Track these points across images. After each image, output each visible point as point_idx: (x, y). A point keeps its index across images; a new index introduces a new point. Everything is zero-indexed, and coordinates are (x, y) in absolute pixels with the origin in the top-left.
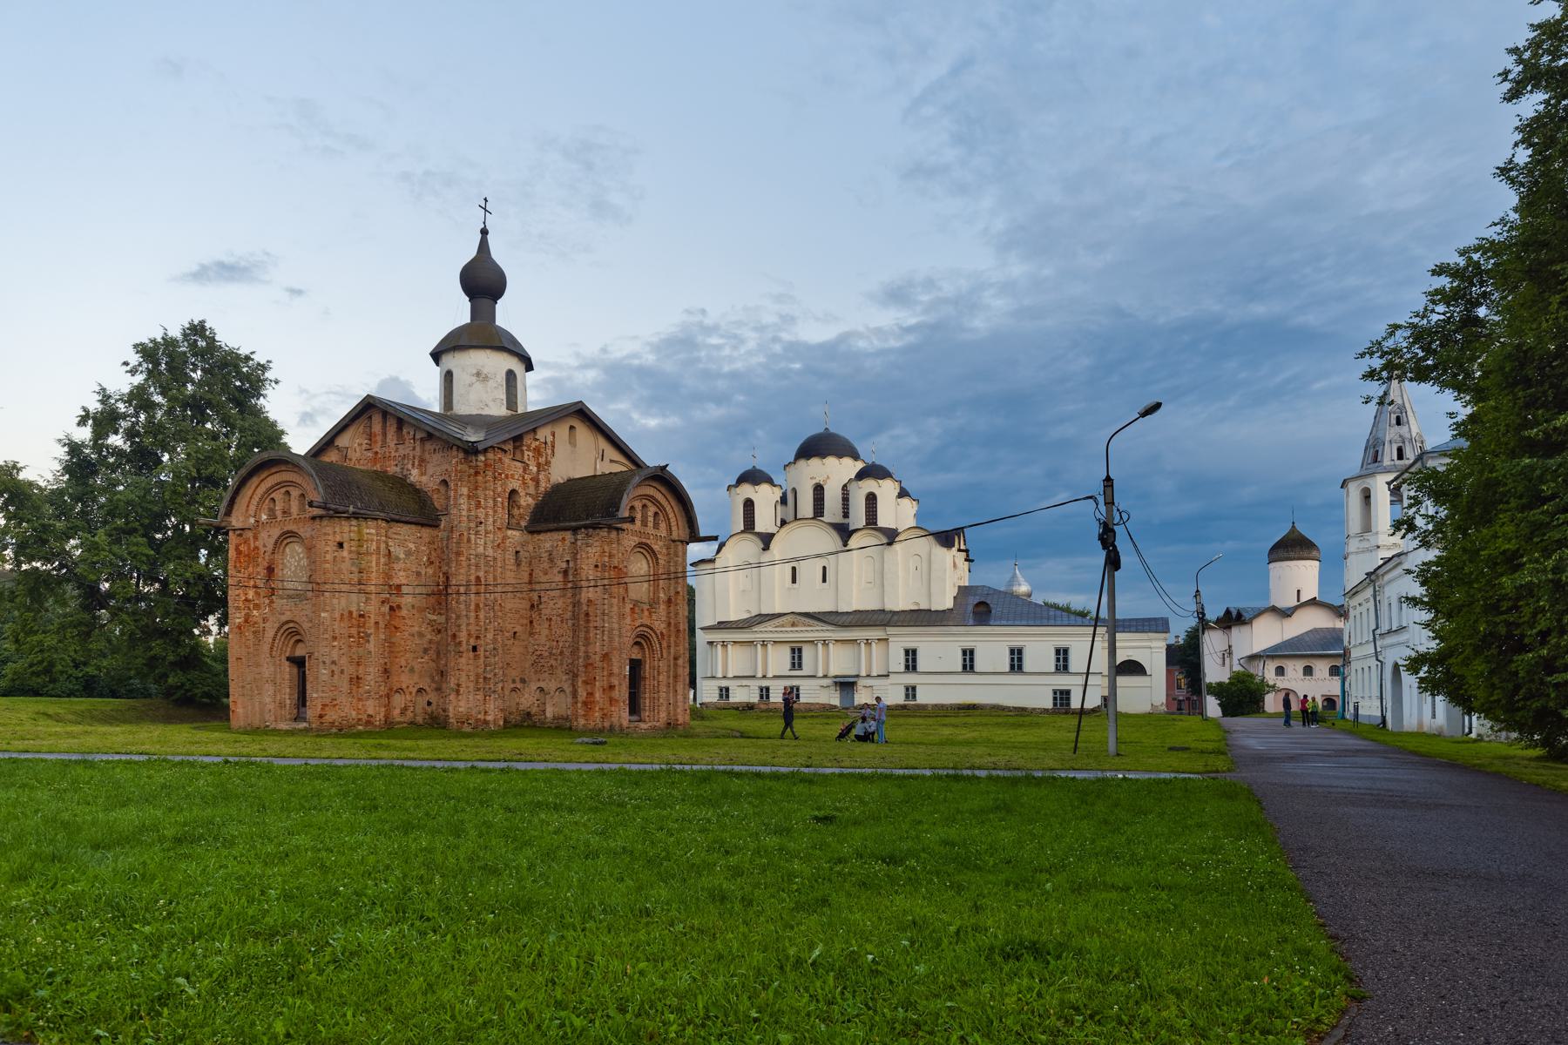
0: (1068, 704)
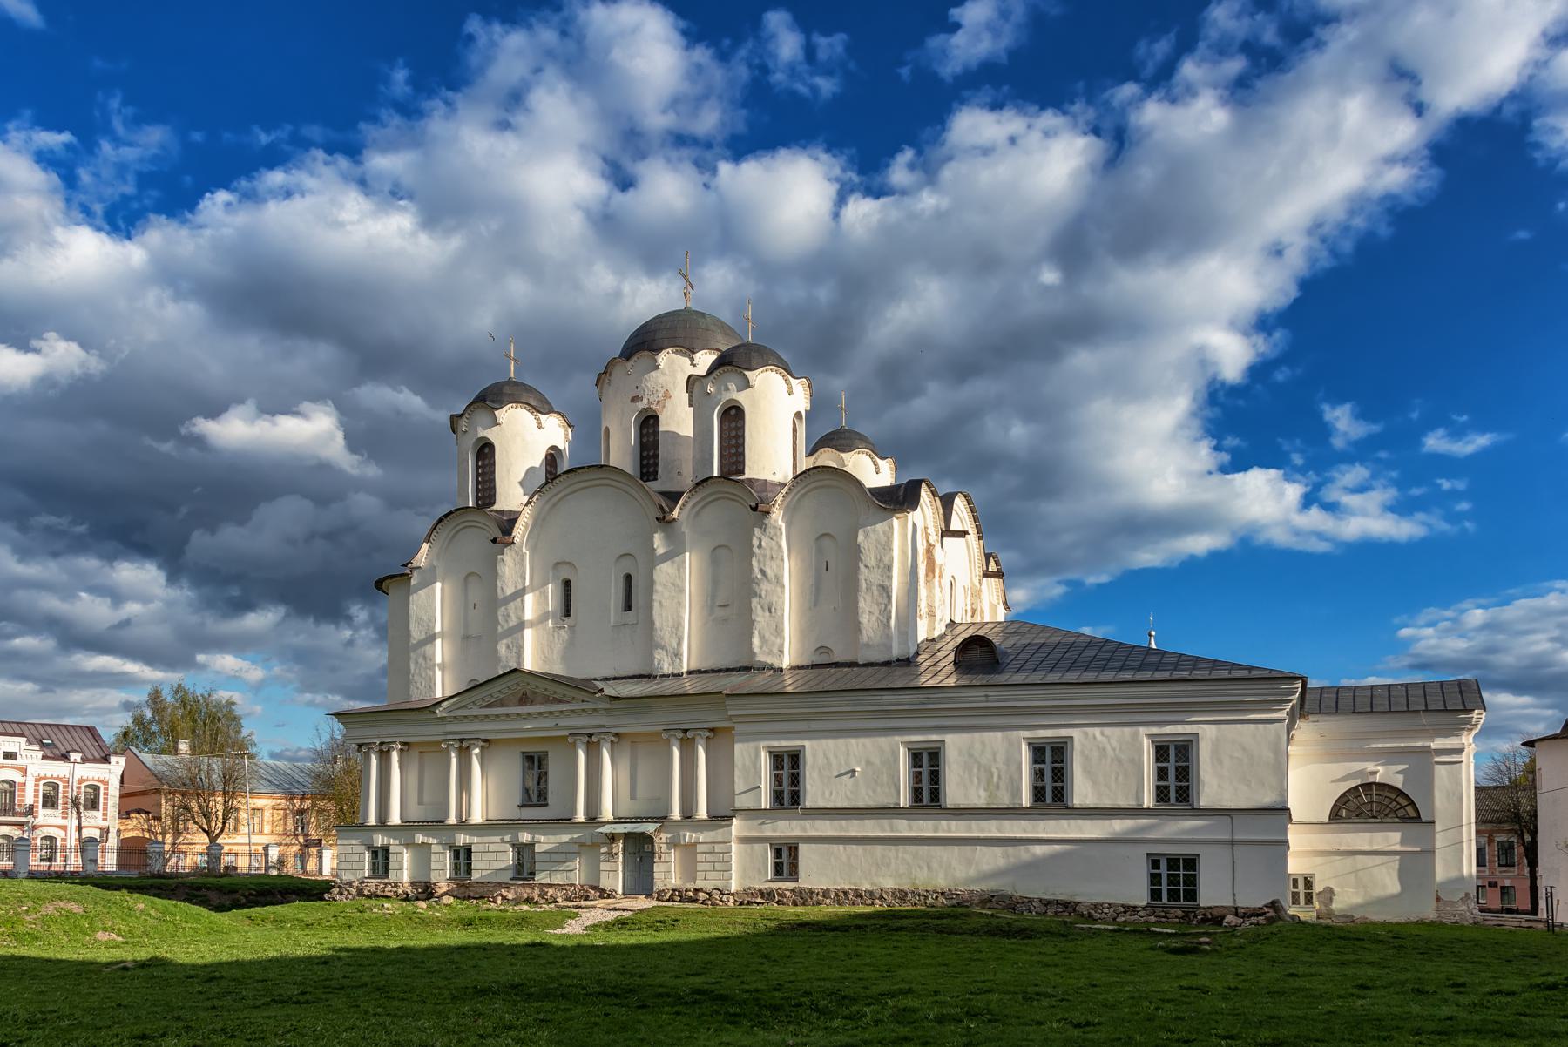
0: (1192, 895)
